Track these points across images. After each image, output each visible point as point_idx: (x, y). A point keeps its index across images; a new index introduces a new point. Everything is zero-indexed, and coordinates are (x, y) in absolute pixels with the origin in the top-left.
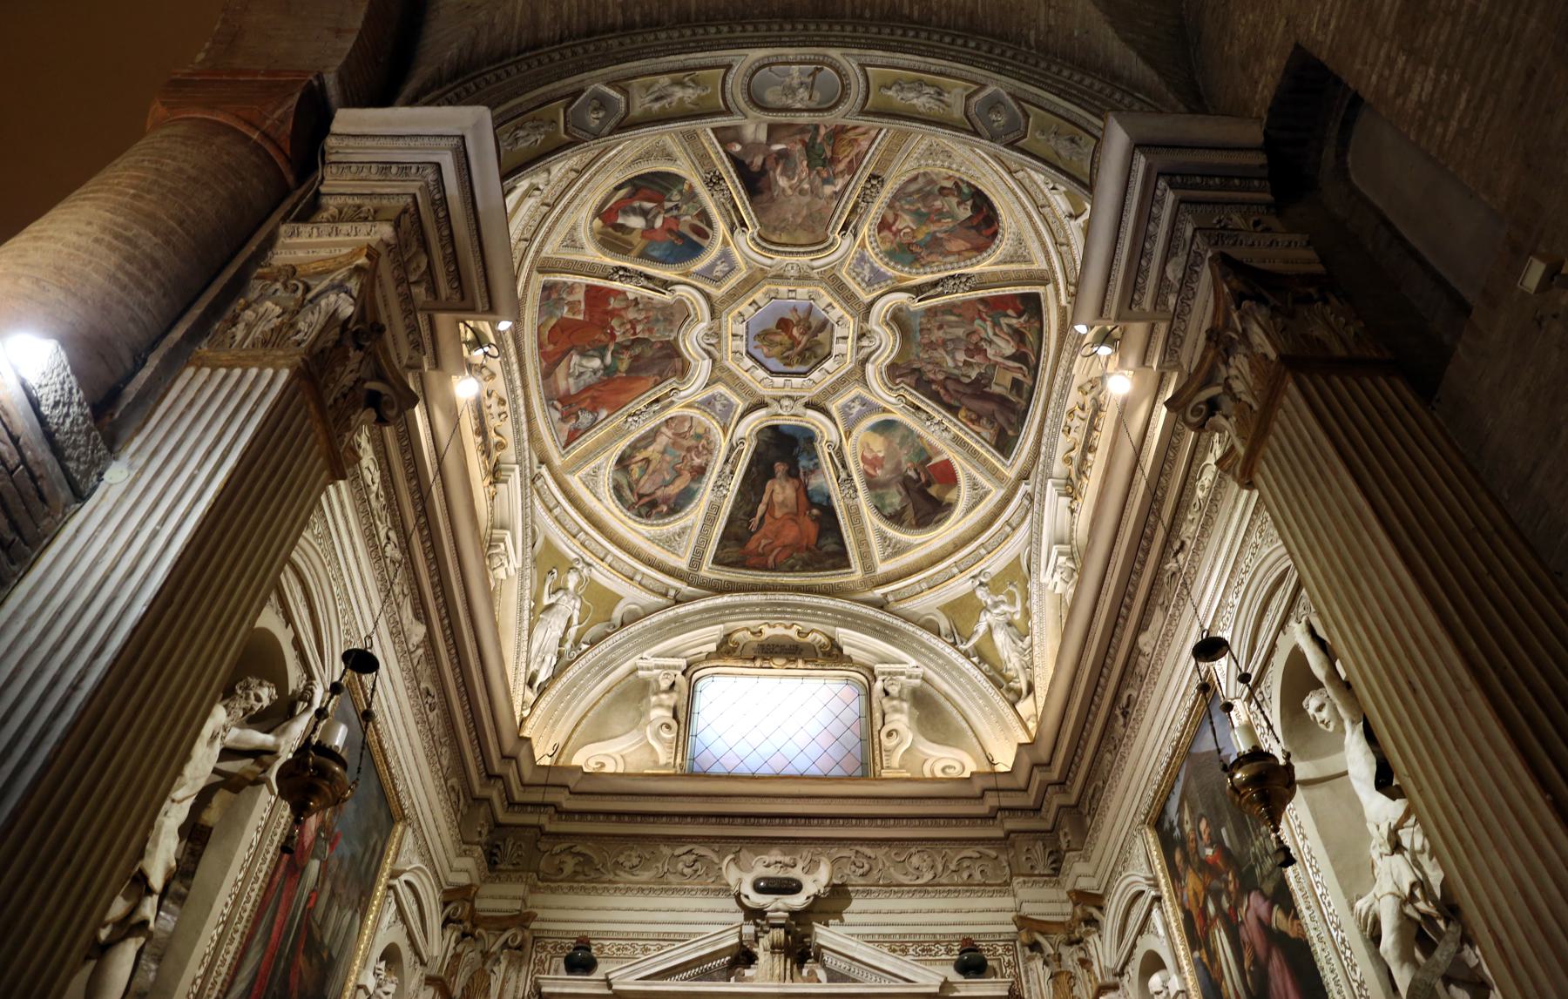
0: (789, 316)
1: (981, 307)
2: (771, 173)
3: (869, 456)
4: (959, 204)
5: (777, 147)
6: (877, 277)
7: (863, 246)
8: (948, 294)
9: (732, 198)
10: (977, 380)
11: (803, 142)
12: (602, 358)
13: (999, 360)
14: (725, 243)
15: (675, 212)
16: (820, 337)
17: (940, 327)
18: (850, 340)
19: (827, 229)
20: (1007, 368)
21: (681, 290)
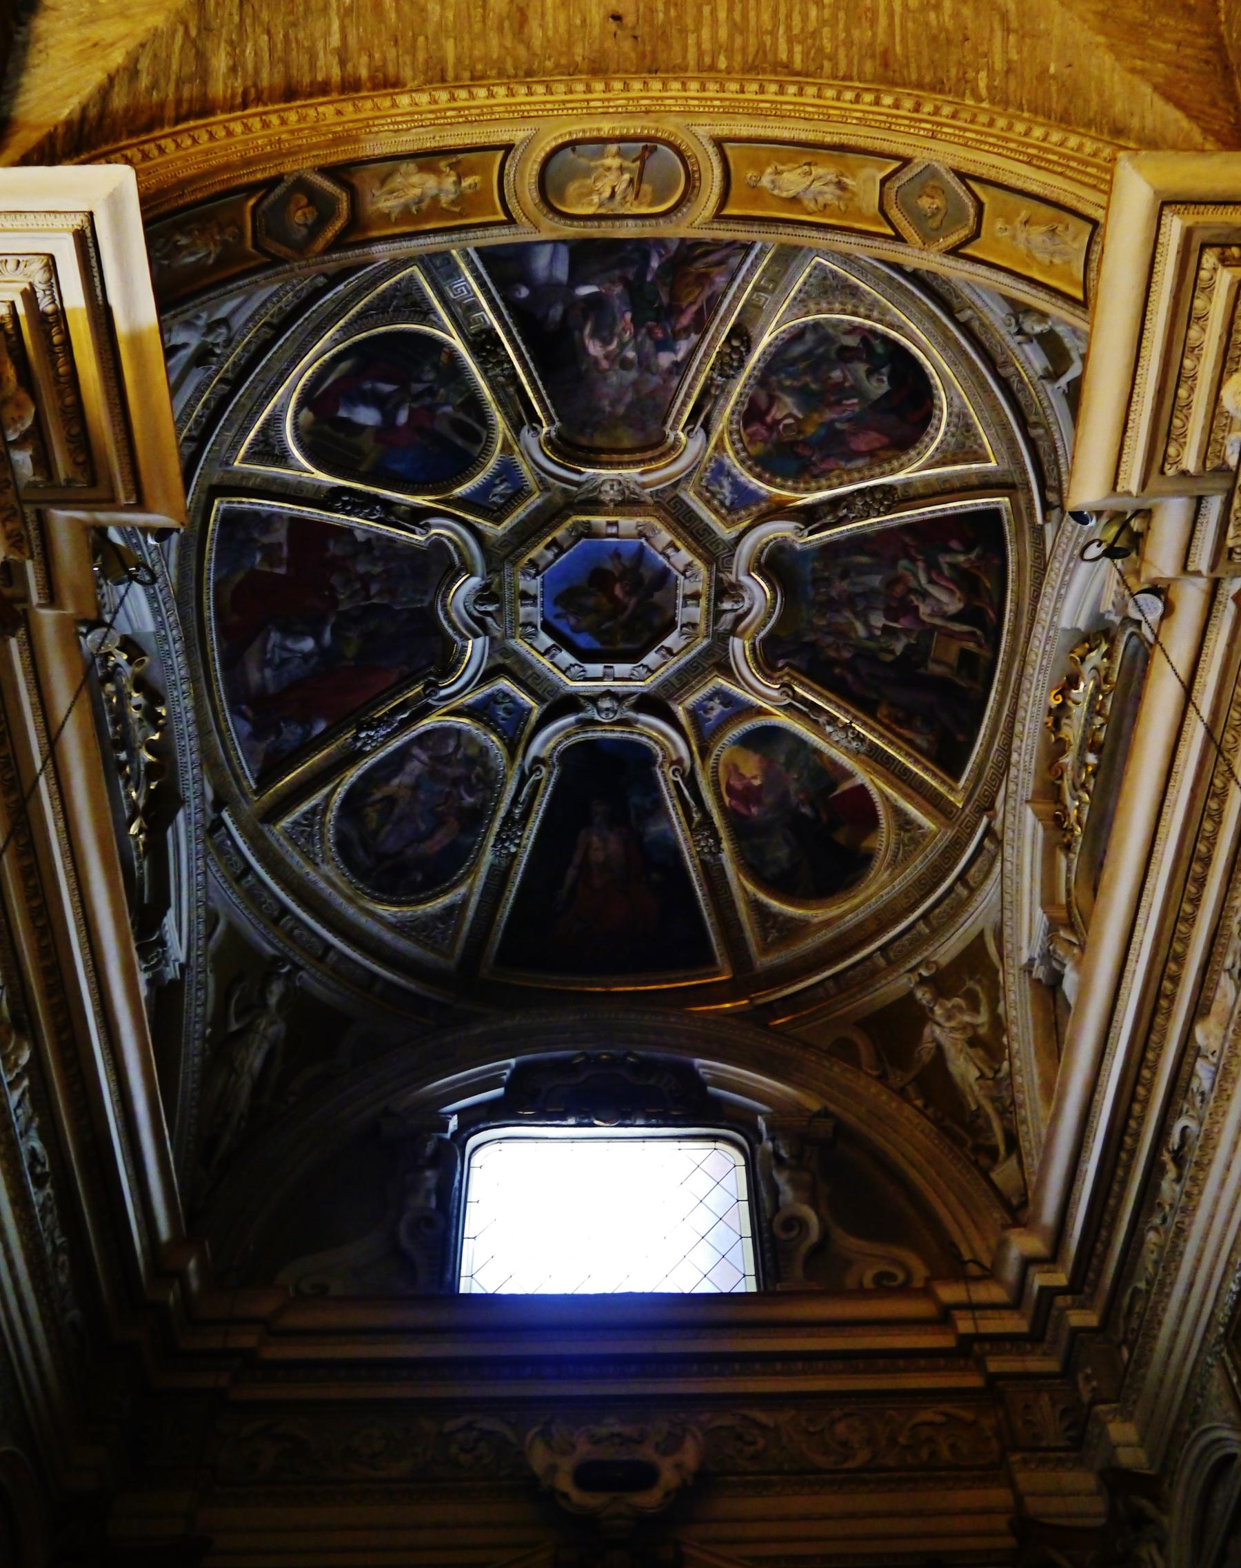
0: (609, 565)
1: (907, 539)
2: (577, 334)
3: (738, 785)
4: (869, 373)
5: (584, 291)
6: (744, 496)
7: (719, 447)
8: (855, 519)
10: (902, 653)
11: (624, 280)
12: (318, 638)
13: (938, 621)
14: (506, 447)
15: (428, 400)
16: (658, 597)
17: (844, 575)
18: (703, 602)
19: (665, 423)
20: (952, 635)
21: (440, 529)
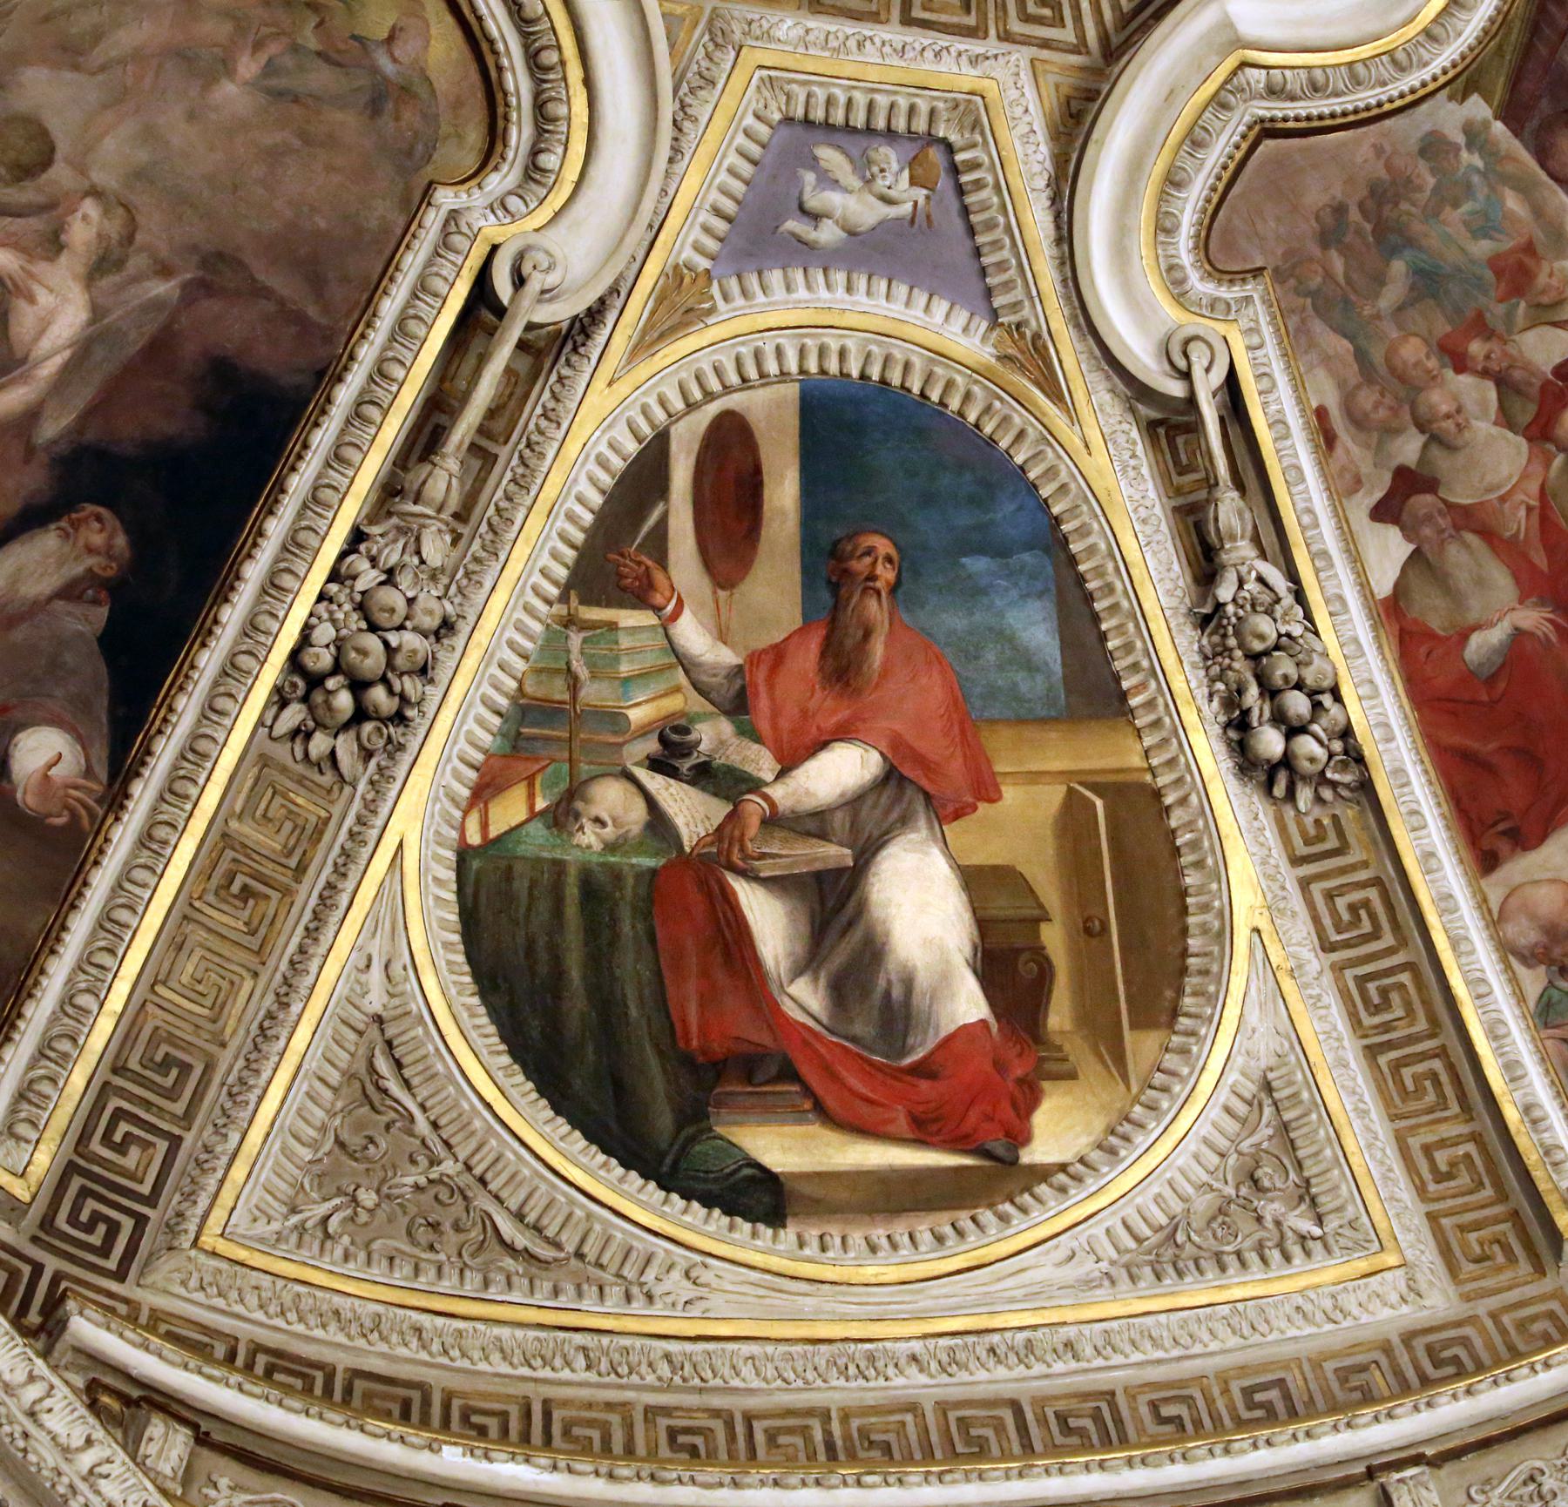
2: (51, 429)
9: (390, 491)
